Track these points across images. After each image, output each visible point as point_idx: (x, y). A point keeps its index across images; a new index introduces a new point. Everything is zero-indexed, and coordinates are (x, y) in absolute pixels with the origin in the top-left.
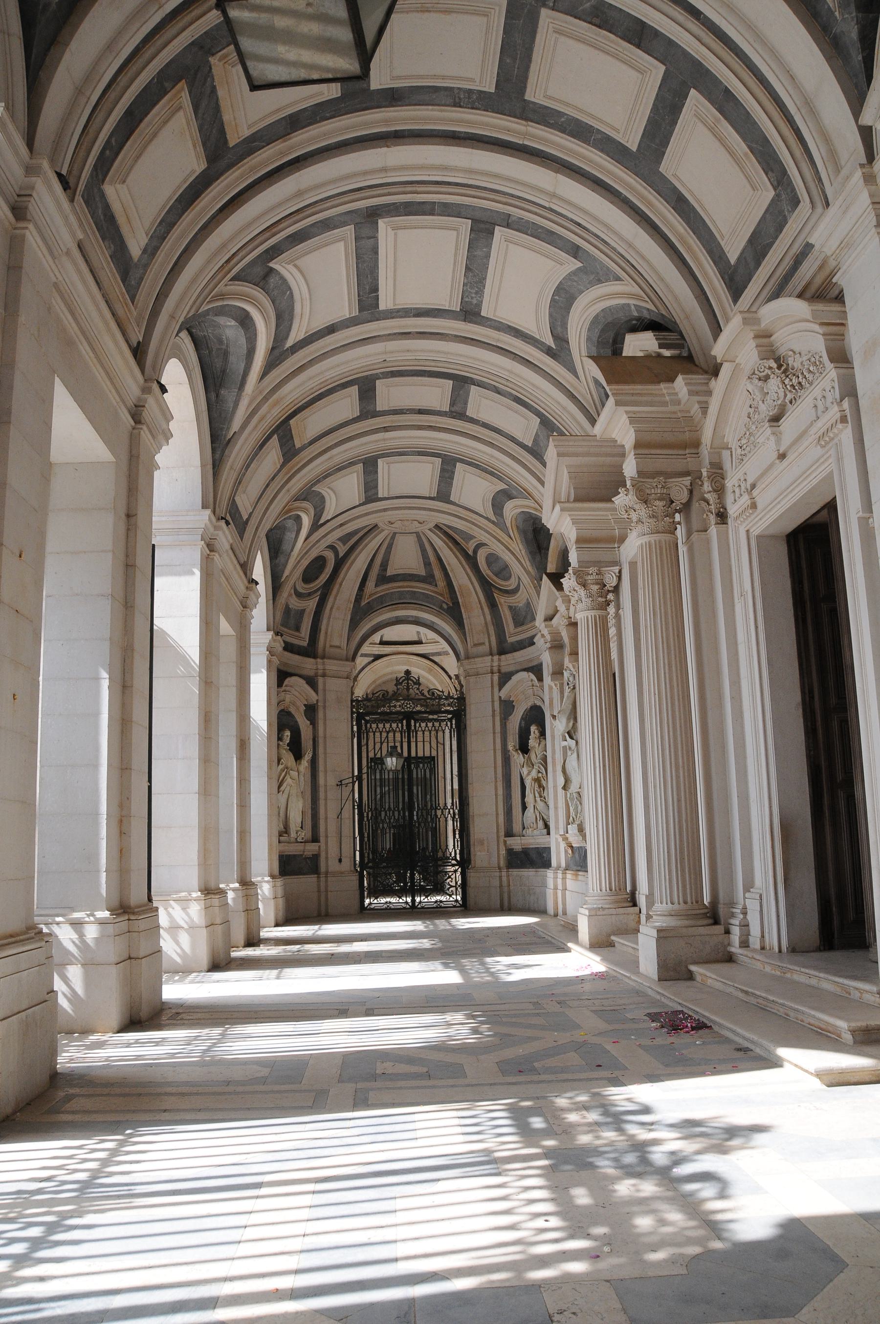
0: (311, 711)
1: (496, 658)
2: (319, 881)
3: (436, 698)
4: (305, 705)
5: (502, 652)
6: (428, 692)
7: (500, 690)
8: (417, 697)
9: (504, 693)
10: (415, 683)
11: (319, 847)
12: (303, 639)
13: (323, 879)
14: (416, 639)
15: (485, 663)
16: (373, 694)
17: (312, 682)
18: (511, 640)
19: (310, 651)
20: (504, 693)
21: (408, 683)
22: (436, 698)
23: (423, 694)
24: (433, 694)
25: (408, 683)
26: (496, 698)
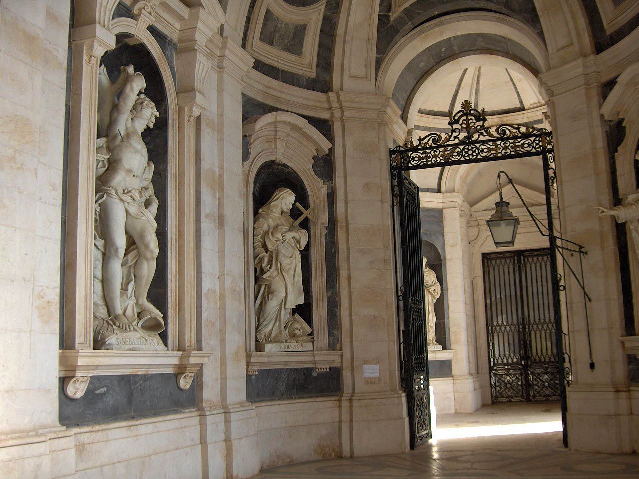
0: (325, 165)
1: (592, 57)
2: (340, 406)
3: (508, 138)
4: (314, 158)
5: (599, 48)
6: (497, 130)
7: (600, 106)
8: (482, 138)
9: (608, 108)
10: (478, 120)
11: (342, 355)
12: (305, 63)
13: (345, 404)
14: (518, 105)
15: (575, 69)
16: (420, 140)
17: (324, 126)
18: (609, 29)
19: (321, 83)
20: (608, 108)
21: (467, 120)
22: (508, 138)
23: (489, 134)
24: (504, 132)
25: (467, 120)
26: (597, 122)
